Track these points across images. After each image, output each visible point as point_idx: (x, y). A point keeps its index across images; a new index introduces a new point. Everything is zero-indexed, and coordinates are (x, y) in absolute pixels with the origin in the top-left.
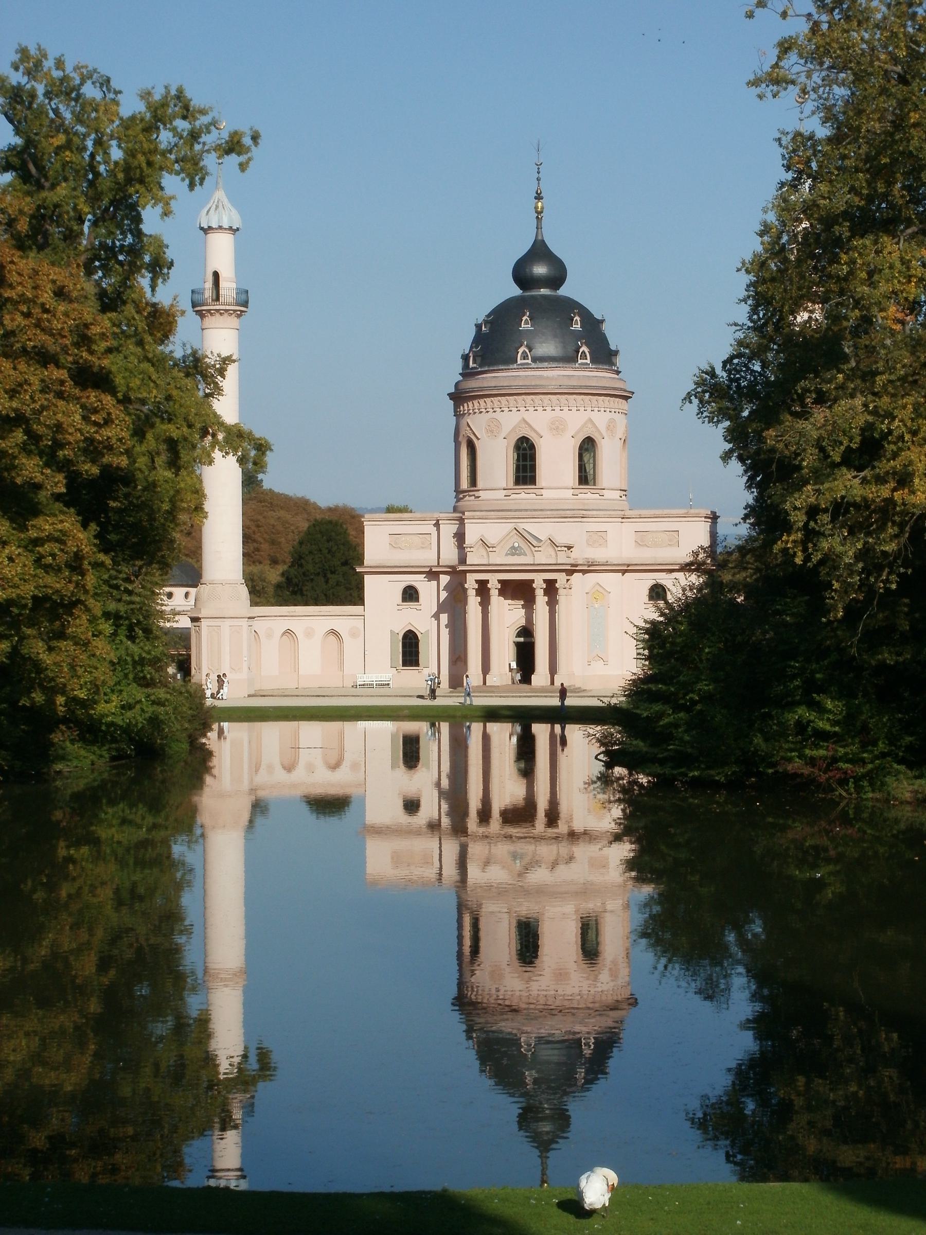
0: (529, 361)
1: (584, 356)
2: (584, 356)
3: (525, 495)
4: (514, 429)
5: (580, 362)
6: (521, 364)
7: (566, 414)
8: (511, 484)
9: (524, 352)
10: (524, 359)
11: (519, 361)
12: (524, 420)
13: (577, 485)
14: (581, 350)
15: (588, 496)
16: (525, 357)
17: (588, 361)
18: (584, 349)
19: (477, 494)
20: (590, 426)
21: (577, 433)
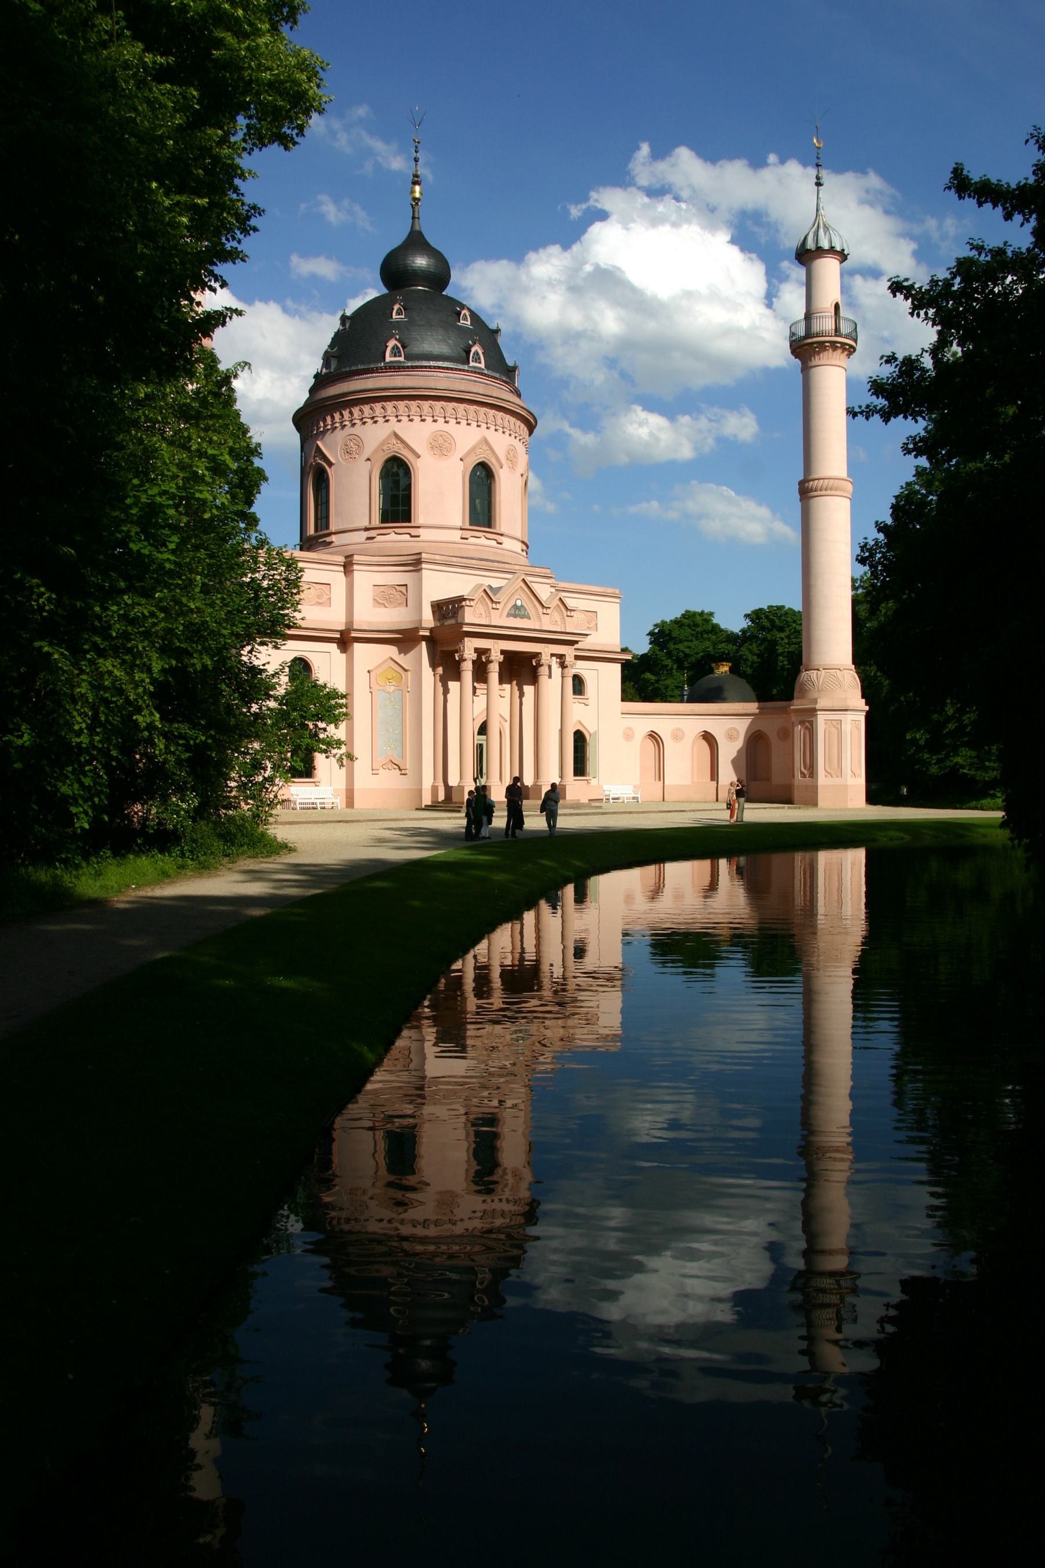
0: (402, 359)
1: (477, 359)
2: (477, 359)
3: (395, 539)
4: (380, 448)
5: (472, 364)
6: (391, 362)
7: (452, 426)
8: (376, 521)
9: (395, 347)
10: (395, 356)
11: (388, 359)
12: (396, 436)
13: (467, 526)
14: (473, 350)
15: (481, 542)
16: (395, 352)
17: (482, 365)
18: (476, 348)
19: (328, 539)
20: (485, 447)
21: (468, 454)
